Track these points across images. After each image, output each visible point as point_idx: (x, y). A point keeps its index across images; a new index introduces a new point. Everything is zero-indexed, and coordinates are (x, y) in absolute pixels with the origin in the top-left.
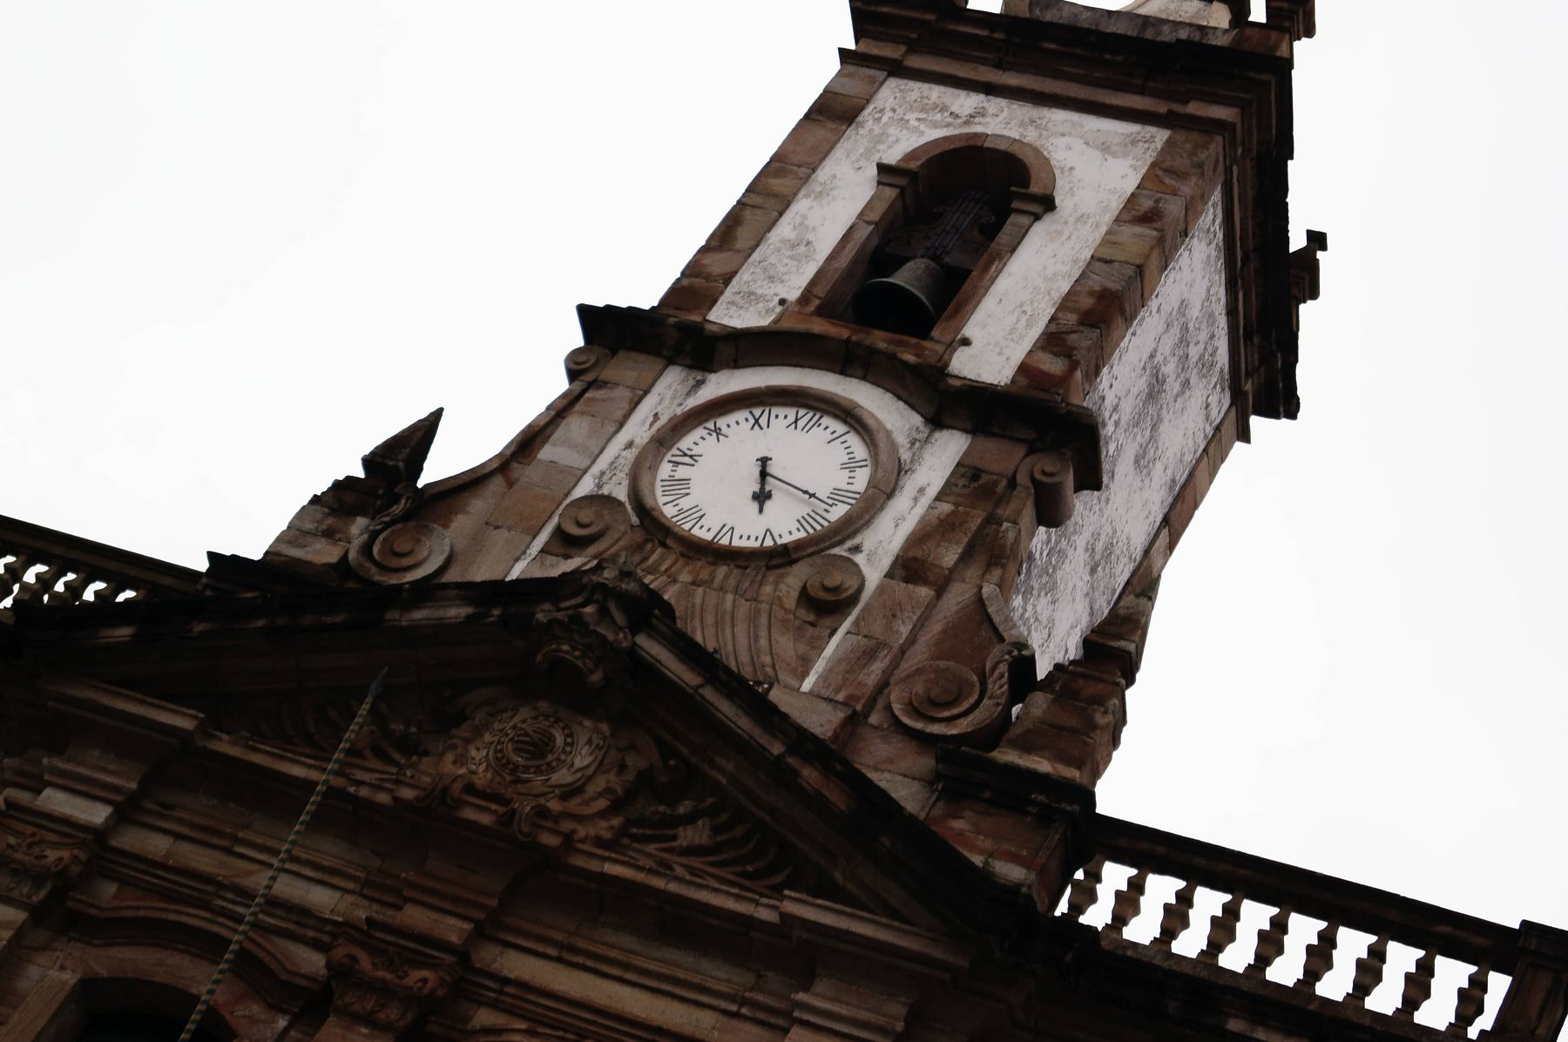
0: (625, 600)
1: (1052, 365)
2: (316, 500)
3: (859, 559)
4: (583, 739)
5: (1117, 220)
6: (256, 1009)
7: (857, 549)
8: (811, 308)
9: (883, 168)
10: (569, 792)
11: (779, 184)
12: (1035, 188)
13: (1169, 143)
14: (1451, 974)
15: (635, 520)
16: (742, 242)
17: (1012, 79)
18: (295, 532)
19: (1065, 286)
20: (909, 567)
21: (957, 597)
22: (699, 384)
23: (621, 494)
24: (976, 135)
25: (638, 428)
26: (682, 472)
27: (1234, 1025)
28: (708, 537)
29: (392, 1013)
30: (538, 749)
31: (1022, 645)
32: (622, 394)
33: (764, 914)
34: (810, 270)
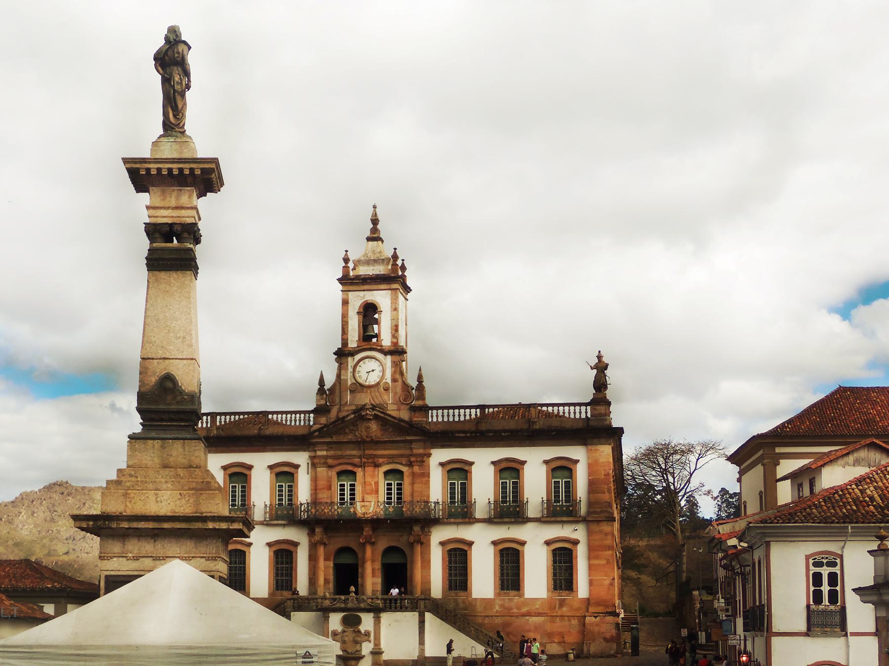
0: (371, 408)
1: (395, 340)
2: (317, 394)
3: (387, 381)
4: (373, 423)
5: (391, 311)
6: (356, 469)
7: (386, 379)
8: (361, 340)
9: (357, 312)
10: (376, 430)
11: (345, 319)
12: (379, 310)
13: (391, 293)
14: (473, 411)
15: (358, 384)
16: (346, 332)
17: (366, 287)
18: (317, 400)
19: (390, 325)
20: (394, 380)
21: (400, 381)
22: (354, 359)
23: (355, 382)
24: (366, 300)
25: (350, 369)
26: (360, 374)
27: (457, 435)
28: (368, 384)
29: (373, 464)
30: (369, 428)
31: (412, 387)
32: (345, 364)
33: (404, 439)
34: (357, 333)
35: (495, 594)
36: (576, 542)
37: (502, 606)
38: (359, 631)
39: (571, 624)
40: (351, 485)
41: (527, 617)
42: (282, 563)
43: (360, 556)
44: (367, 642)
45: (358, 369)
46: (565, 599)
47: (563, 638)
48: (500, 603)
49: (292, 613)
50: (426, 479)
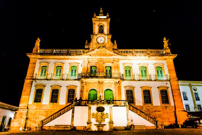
20: (108, 42)
35: (143, 104)
36: (168, 88)
37: (146, 108)
38: (104, 114)
39: (170, 115)
40: (95, 70)
41: (155, 112)
42: (71, 94)
43: (98, 91)
44: (107, 118)
45: (98, 39)
46: (167, 106)
47: (169, 120)
48: (146, 107)
49: (75, 107)
50: (118, 68)
